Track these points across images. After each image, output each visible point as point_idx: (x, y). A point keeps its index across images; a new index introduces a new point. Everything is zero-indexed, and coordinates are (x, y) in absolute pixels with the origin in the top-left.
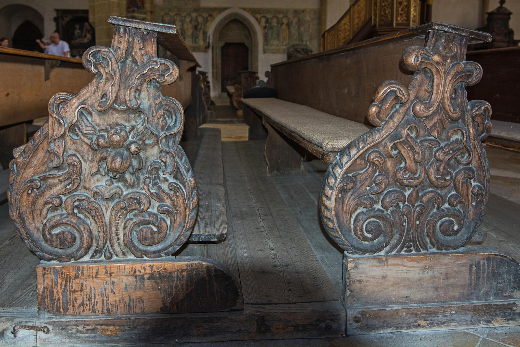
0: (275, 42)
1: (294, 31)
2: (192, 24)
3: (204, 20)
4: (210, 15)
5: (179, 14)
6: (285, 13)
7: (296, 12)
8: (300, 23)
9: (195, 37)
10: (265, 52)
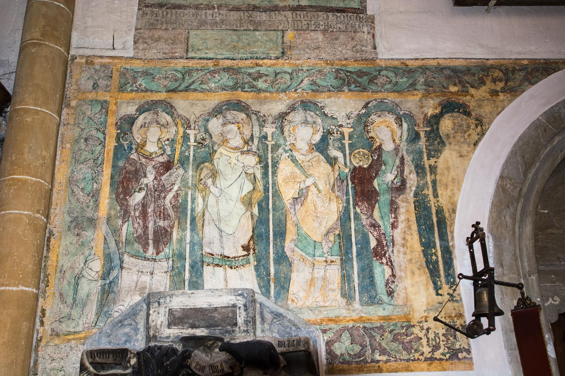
2: (332, 161)
3: (414, 137)
4: (448, 107)
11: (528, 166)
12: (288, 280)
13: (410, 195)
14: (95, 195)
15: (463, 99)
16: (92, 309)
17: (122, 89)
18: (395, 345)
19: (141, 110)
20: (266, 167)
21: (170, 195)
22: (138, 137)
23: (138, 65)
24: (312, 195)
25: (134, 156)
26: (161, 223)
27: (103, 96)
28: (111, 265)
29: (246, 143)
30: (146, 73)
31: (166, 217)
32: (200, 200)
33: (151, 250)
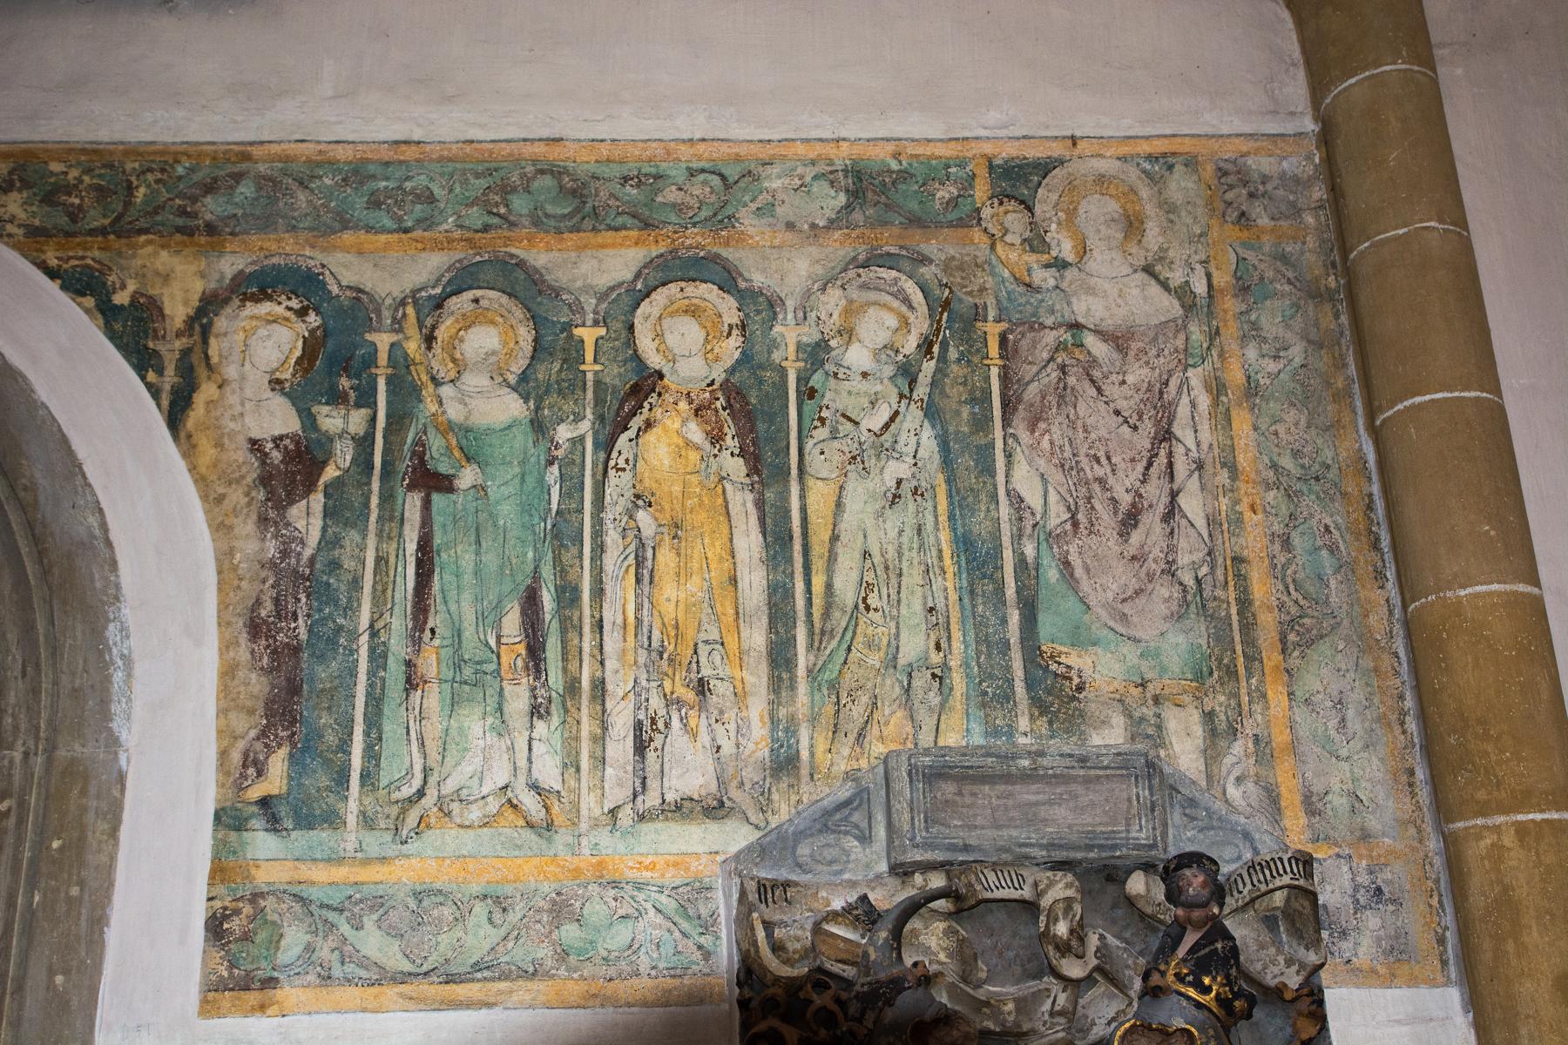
0: (484, 750)
6: (684, 218)
7: (881, 200)
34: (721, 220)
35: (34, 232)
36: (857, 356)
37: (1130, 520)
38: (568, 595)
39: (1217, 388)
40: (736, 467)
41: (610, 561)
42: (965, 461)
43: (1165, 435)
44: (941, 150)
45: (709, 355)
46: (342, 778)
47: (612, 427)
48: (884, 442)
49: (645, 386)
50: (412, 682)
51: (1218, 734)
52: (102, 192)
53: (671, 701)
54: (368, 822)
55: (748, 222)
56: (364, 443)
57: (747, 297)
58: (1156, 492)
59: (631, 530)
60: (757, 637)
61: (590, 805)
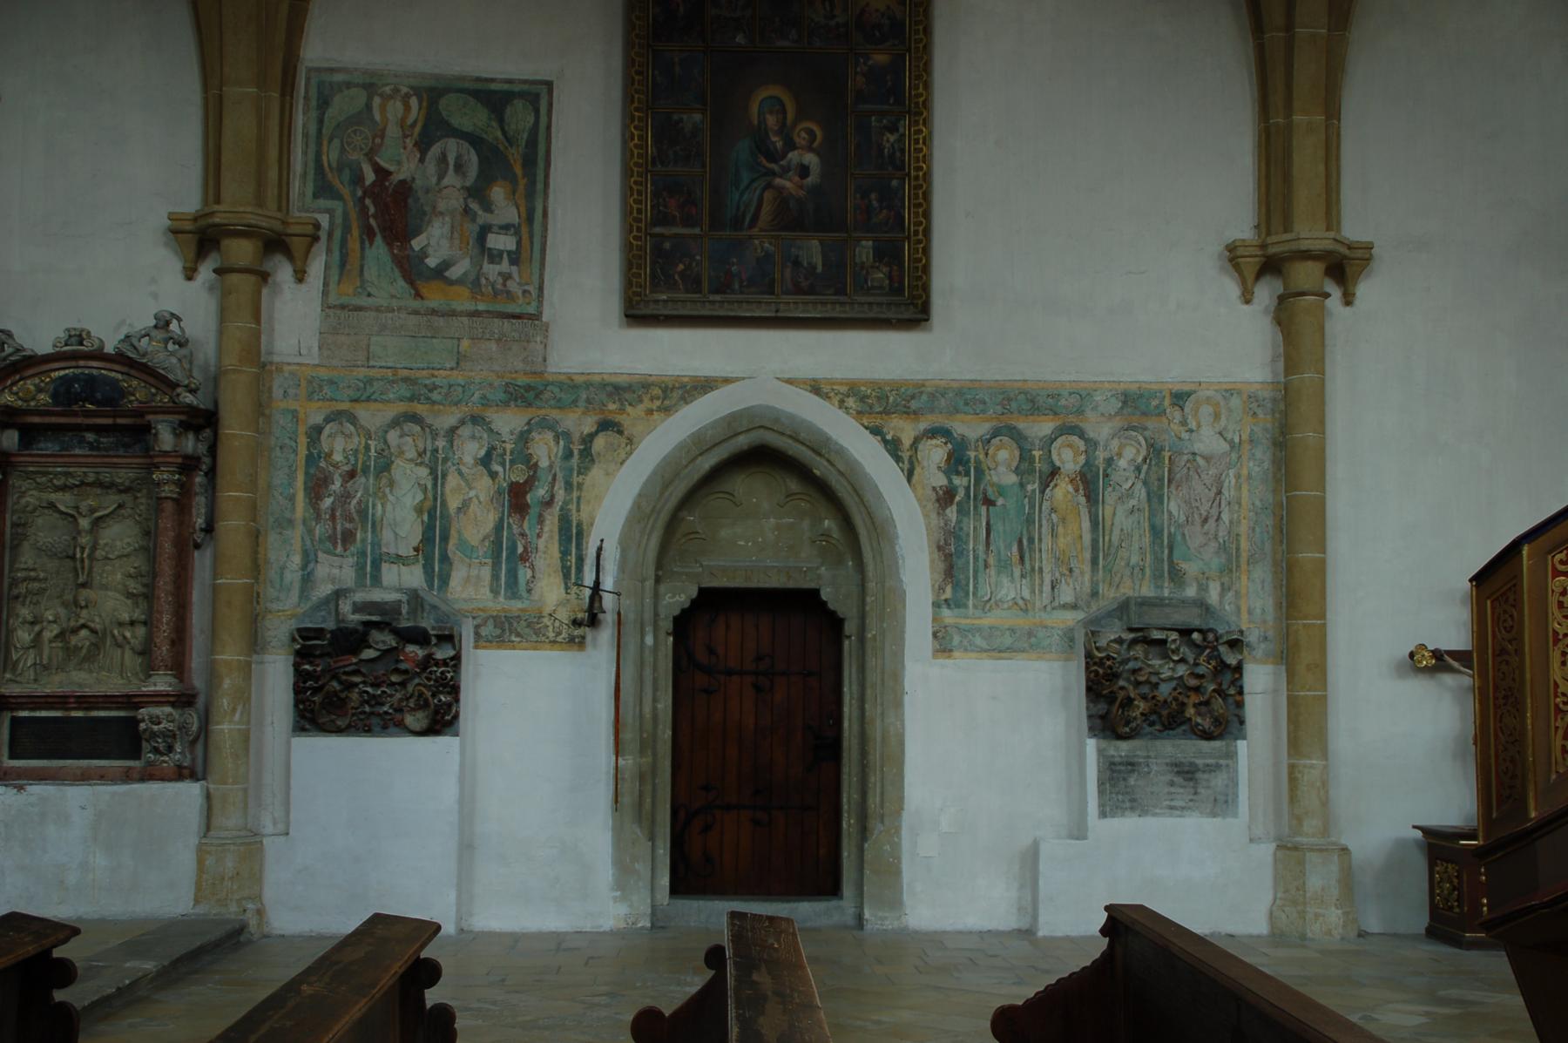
0: (1008, 589)
1: (1121, 516)
2: (493, 475)
3: (568, 455)
4: (605, 425)
5: (415, 418)
6: (1066, 409)
7: (1135, 405)
8: (1162, 468)
9: (509, 558)
10: (943, 644)
11: (666, 486)
12: (449, 576)
13: (556, 509)
14: (292, 499)
15: (618, 418)
16: (295, 593)
17: (310, 398)
18: (527, 630)
19: (328, 420)
20: (435, 479)
21: (354, 502)
22: (325, 445)
23: (323, 373)
24: (473, 507)
25: (323, 464)
26: (348, 525)
27: (294, 405)
28: (308, 559)
29: (420, 455)
30: (331, 382)
31: (351, 520)
32: (379, 507)
33: (339, 549)
34: (1080, 412)
35: (859, 413)
36: (1122, 463)
37: (1205, 520)
38: (1031, 540)
39: (1238, 477)
40: (1083, 500)
41: (1044, 530)
42: (1155, 500)
43: (1219, 493)
44: (1154, 387)
45: (1075, 462)
46: (967, 594)
47: (1044, 486)
48: (1129, 494)
49: (1055, 472)
50: (986, 566)
51: (1224, 589)
52: (879, 398)
53: (1062, 575)
54: (975, 607)
55: (1089, 414)
56: (967, 489)
57: (1087, 441)
58: (1214, 512)
59: (1049, 520)
60: (1088, 555)
61: (1038, 604)
